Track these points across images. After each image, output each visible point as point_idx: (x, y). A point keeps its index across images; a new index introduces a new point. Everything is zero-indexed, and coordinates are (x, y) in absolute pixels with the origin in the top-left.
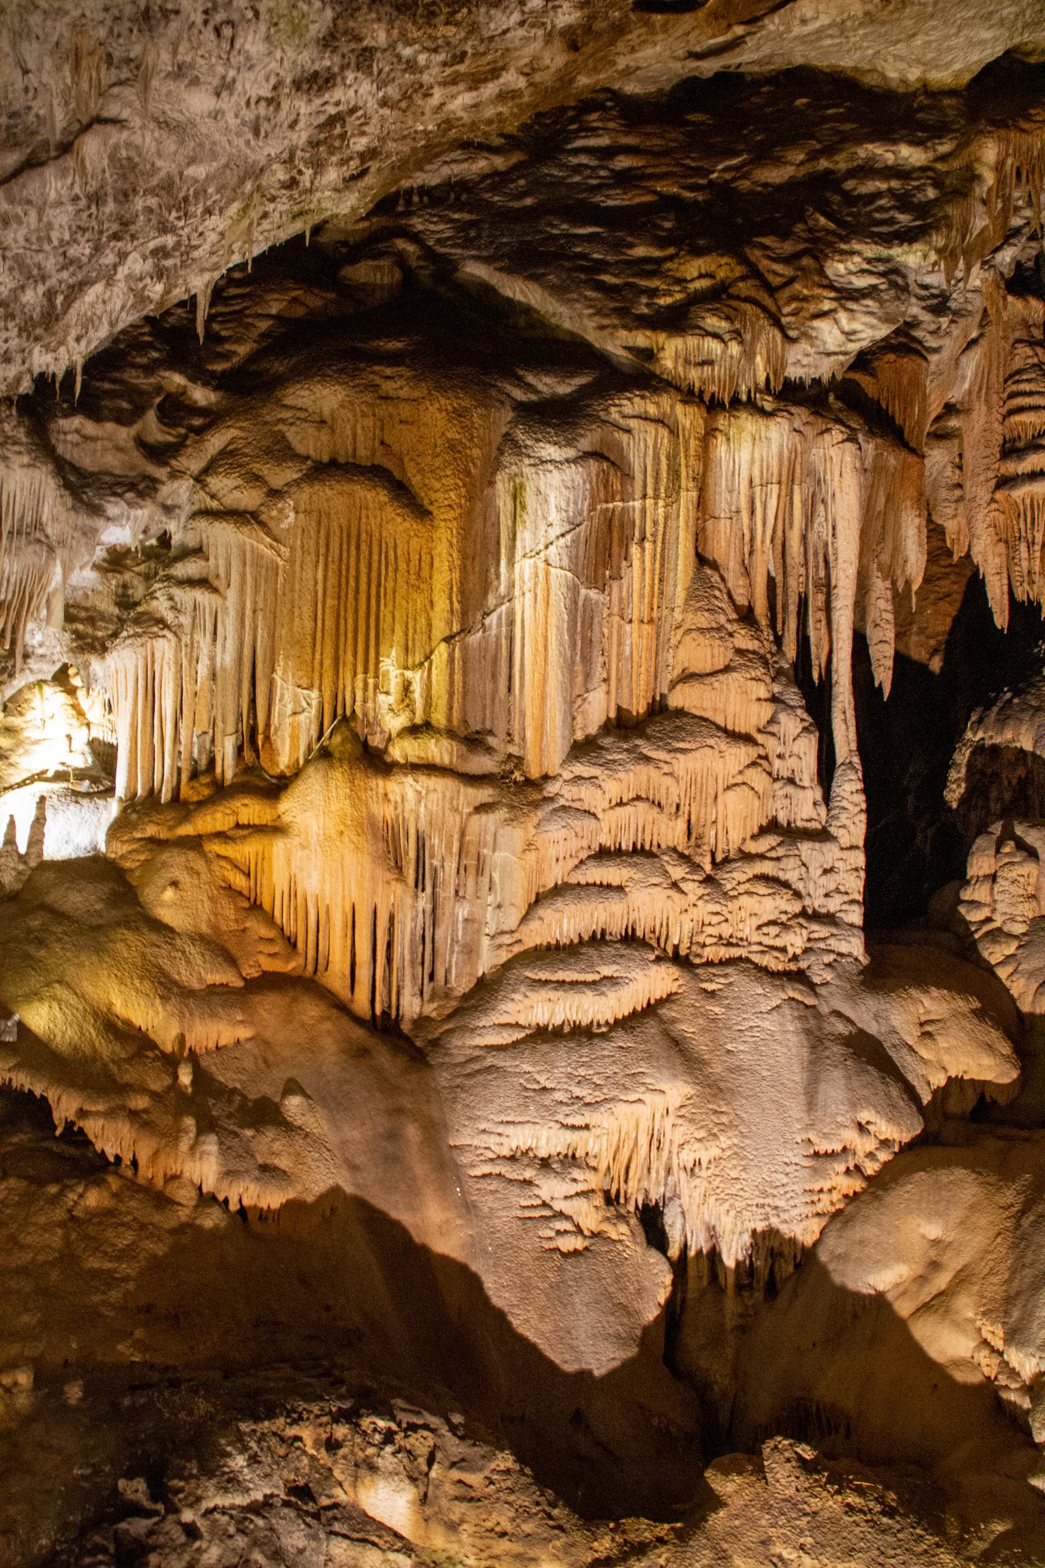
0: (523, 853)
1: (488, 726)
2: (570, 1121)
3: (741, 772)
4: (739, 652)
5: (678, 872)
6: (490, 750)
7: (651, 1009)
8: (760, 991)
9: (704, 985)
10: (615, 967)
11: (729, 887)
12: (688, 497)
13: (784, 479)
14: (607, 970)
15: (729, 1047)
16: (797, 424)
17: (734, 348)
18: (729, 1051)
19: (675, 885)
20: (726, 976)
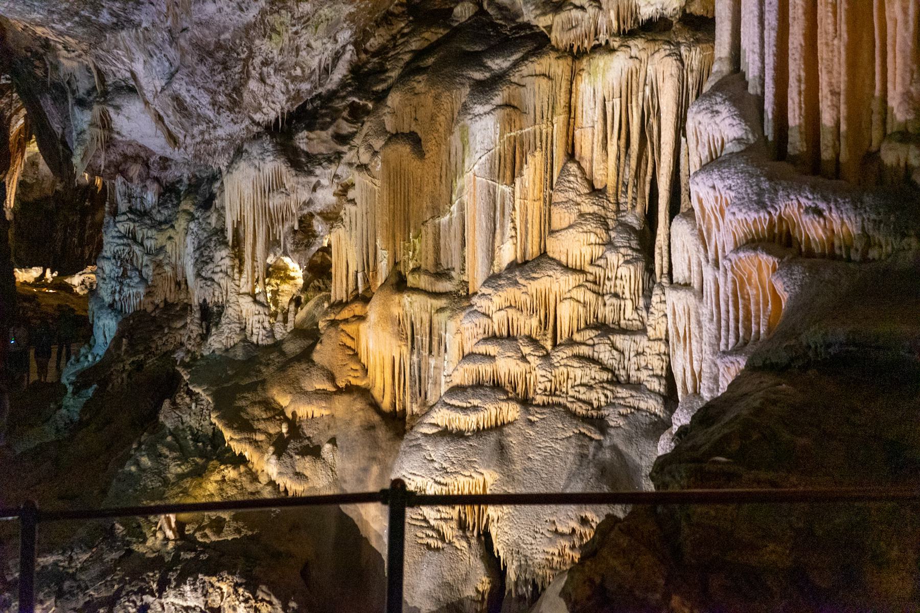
0: (460, 332)
1: (450, 266)
2: (438, 479)
3: (569, 291)
4: (581, 215)
5: (526, 350)
6: (451, 278)
7: (499, 427)
8: (560, 426)
9: (530, 417)
10: (479, 401)
11: (555, 360)
12: (560, 120)
13: (624, 94)
14: (476, 402)
15: (530, 455)
16: (634, 52)
17: (591, 11)
18: (529, 458)
19: (524, 358)
20: (541, 414)
